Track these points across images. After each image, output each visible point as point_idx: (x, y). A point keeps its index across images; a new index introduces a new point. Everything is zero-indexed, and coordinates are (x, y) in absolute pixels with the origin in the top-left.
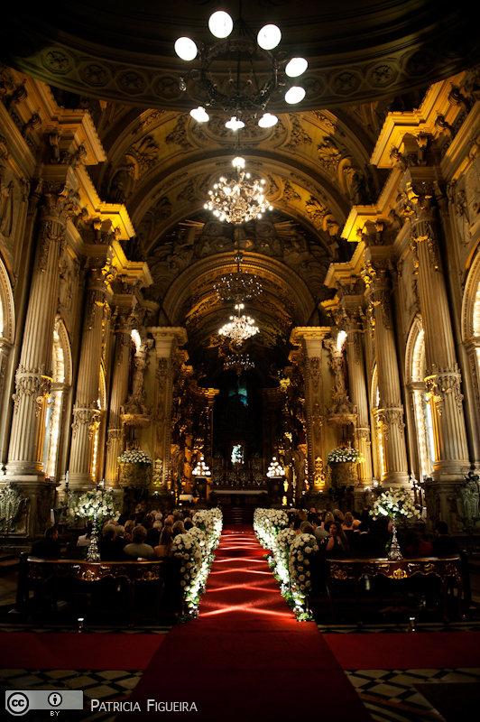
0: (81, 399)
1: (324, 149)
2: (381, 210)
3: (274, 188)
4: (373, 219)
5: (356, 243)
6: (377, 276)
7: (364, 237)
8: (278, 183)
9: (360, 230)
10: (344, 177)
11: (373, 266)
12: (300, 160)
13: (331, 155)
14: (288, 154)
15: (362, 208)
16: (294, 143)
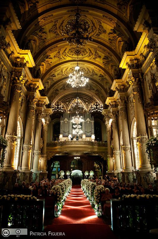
0: (9, 130)
1: (111, 34)
2: (136, 53)
3: (91, 54)
4: (133, 57)
5: (125, 69)
6: (135, 80)
7: (130, 67)
8: (92, 52)
9: (127, 63)
10: (119, 46)
11: (133, 76)
12: (102, 41)
13: (113, 37)
14: (96, 39)
15: (128, 53)
16: (99, 34)
